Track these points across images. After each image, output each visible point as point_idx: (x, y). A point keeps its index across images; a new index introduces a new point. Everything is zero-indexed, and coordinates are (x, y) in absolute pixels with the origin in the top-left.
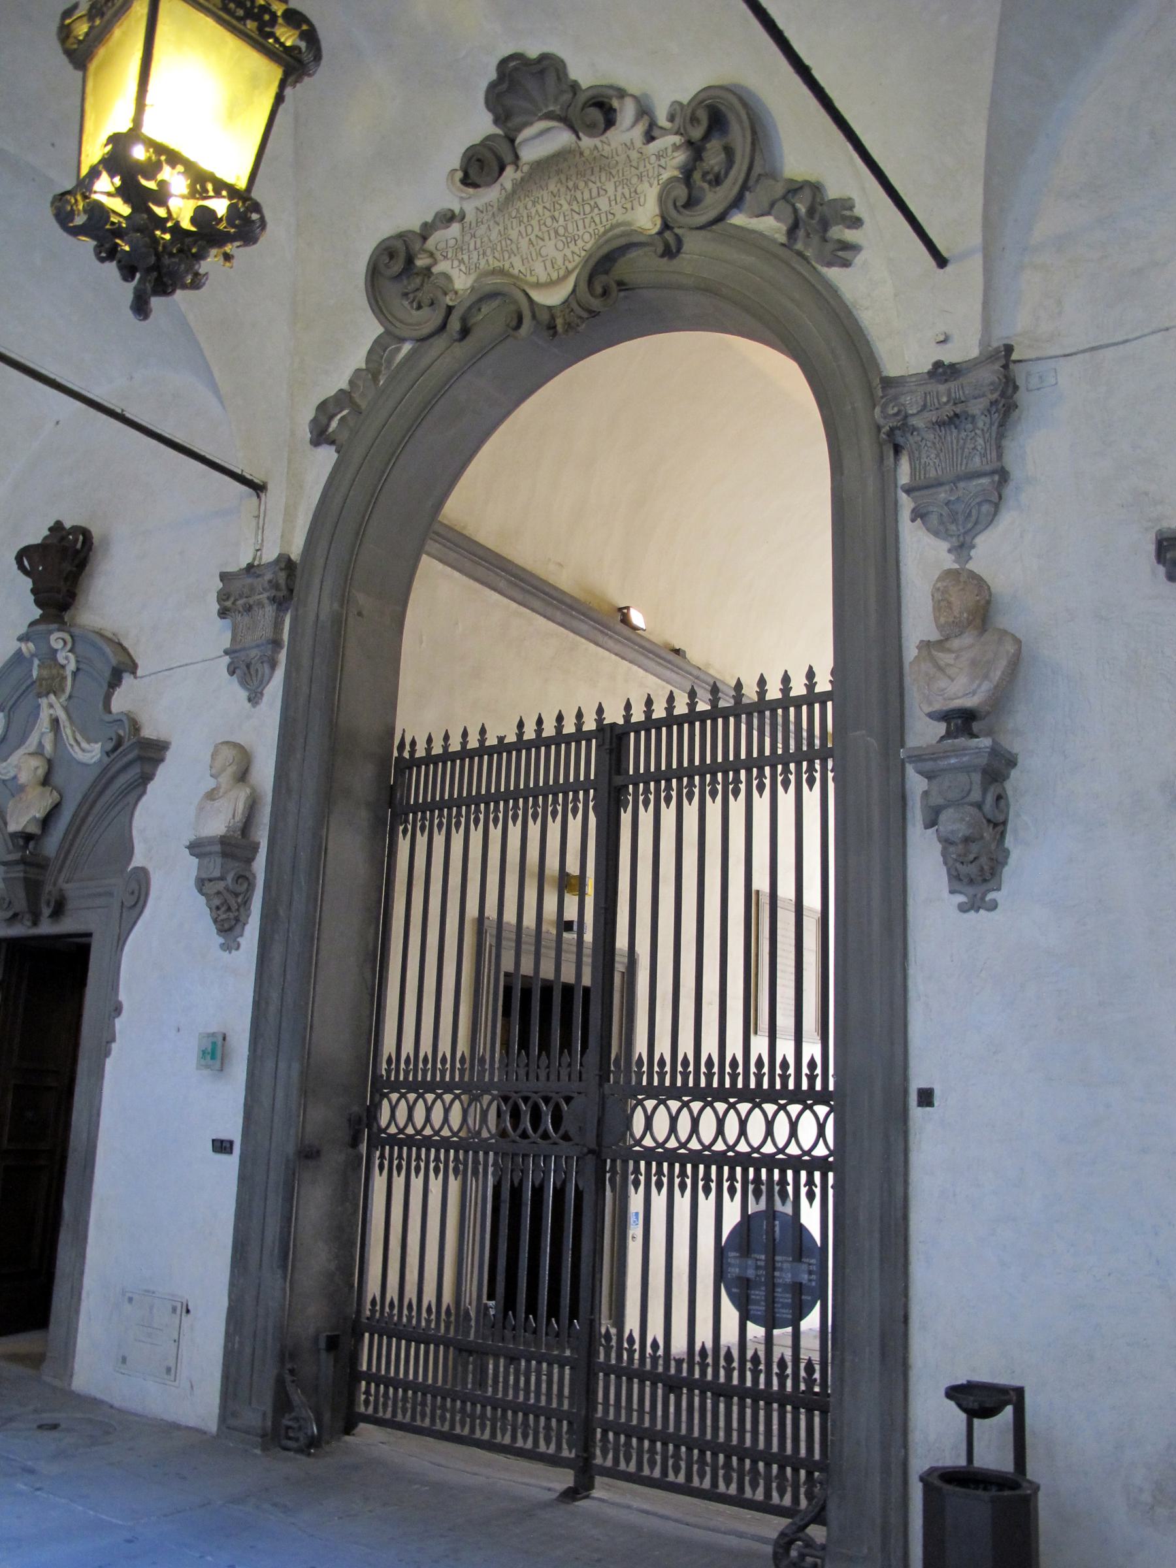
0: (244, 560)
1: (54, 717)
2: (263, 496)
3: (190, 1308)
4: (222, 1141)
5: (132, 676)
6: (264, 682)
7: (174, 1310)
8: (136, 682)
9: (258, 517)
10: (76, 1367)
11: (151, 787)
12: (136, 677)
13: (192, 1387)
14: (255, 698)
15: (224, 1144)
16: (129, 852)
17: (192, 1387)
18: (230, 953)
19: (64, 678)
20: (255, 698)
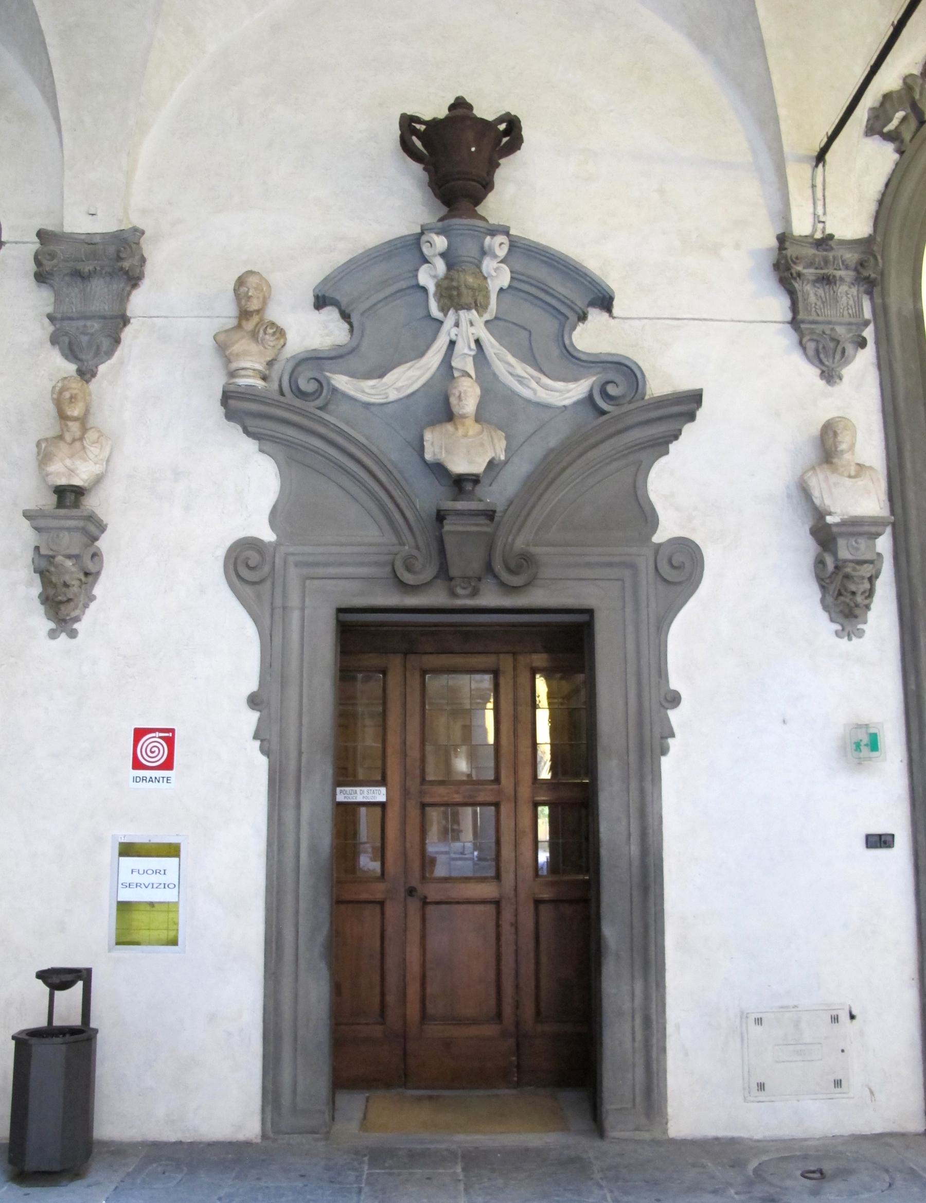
0: (802, 226)
1: (476, 338)
2: (821, 165)
3: (854, 1013)
4: (880, 836)
5: (606, 315)
6: (845, 358)
7: (835, 1019)
8: (612, 321)
9: (813, 186)
10: (670, 1110)
11: (673, 447)
12: (614, 318)
13: (872, 1093)
14: (830, 376)
15: (883, 839)
16: (649, 519)
17: (872, 1093)
18: (850, 639)
19: (487, 297)
20: (830, 376)
